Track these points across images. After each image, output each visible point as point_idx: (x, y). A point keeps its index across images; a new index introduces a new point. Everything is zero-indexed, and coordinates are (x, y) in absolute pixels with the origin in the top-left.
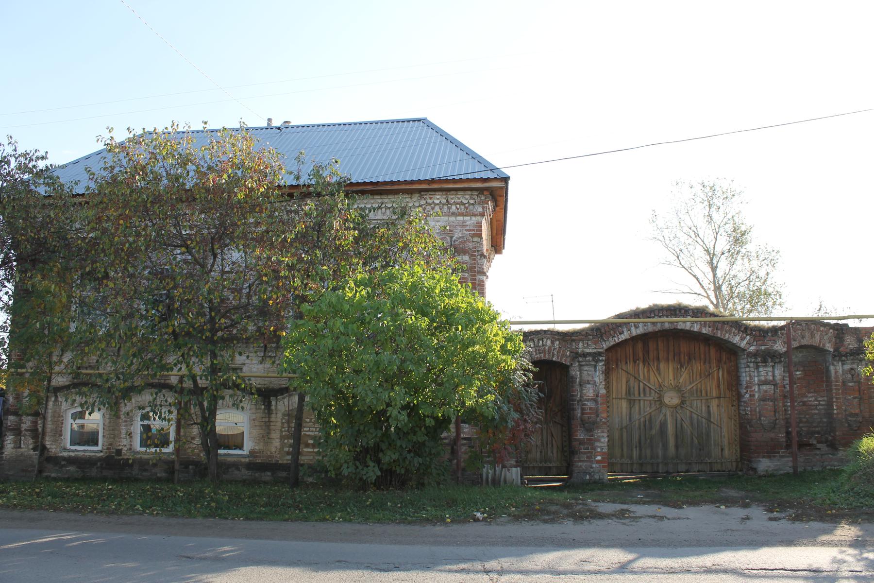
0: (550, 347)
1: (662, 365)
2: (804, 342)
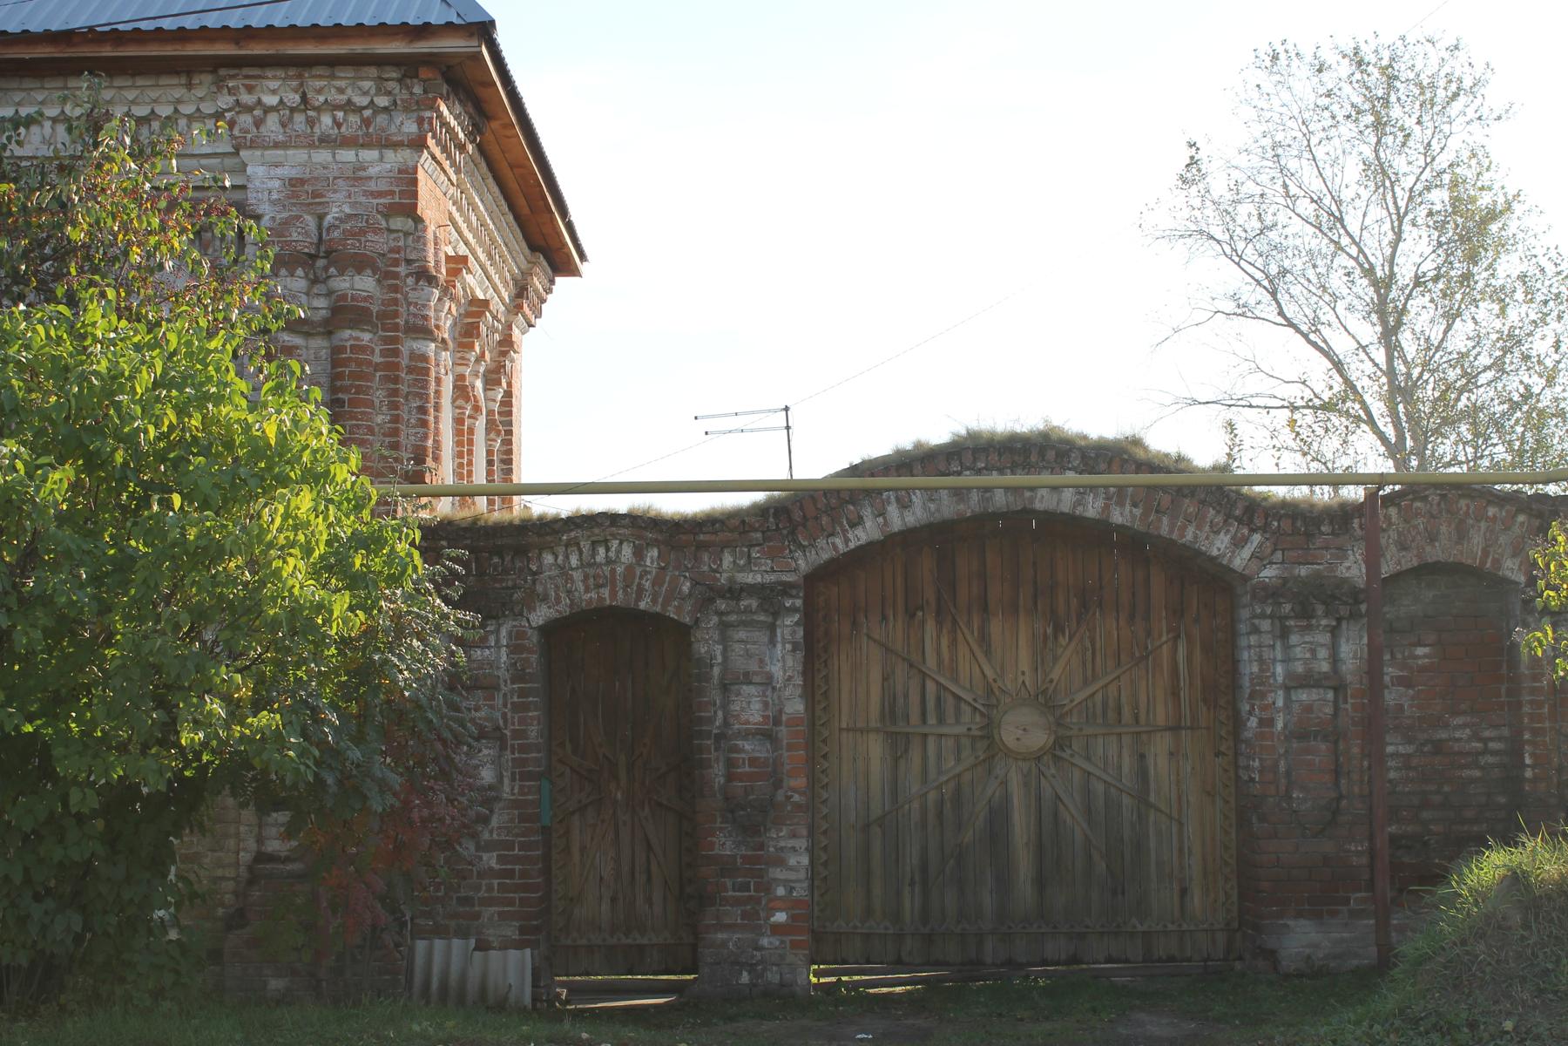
0: (630, 569)
1: (996, 627)
2: (1435, 553)
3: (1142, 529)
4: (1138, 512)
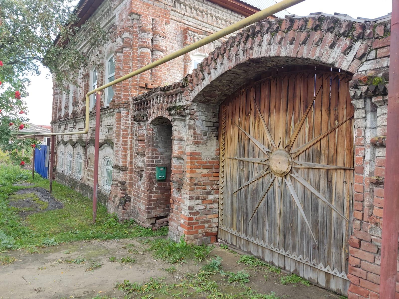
3: (295, 56)
4: (292, 47)
